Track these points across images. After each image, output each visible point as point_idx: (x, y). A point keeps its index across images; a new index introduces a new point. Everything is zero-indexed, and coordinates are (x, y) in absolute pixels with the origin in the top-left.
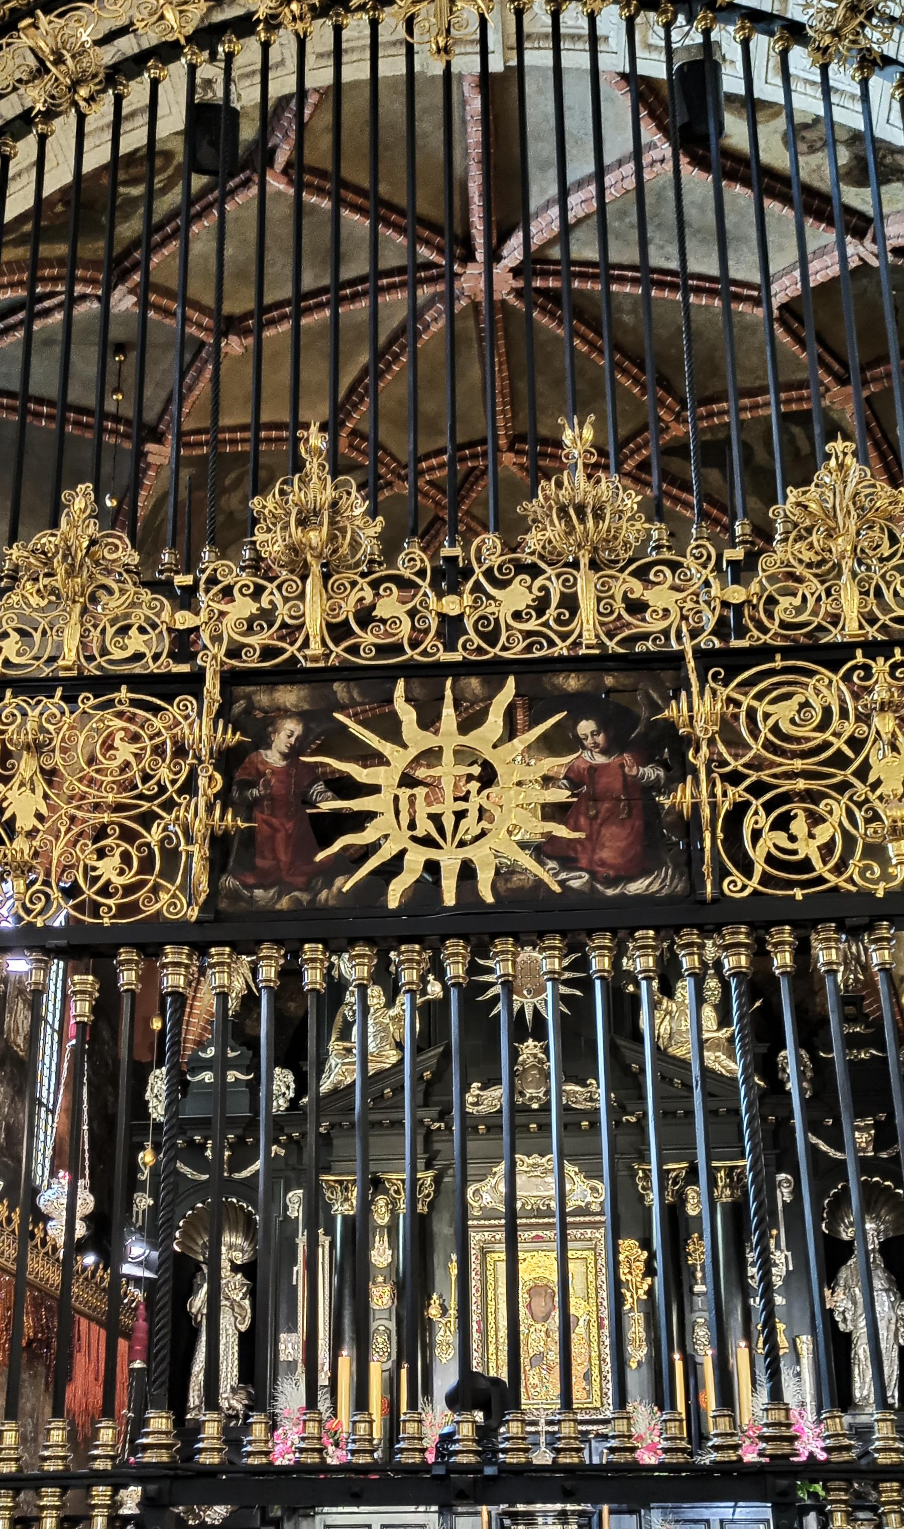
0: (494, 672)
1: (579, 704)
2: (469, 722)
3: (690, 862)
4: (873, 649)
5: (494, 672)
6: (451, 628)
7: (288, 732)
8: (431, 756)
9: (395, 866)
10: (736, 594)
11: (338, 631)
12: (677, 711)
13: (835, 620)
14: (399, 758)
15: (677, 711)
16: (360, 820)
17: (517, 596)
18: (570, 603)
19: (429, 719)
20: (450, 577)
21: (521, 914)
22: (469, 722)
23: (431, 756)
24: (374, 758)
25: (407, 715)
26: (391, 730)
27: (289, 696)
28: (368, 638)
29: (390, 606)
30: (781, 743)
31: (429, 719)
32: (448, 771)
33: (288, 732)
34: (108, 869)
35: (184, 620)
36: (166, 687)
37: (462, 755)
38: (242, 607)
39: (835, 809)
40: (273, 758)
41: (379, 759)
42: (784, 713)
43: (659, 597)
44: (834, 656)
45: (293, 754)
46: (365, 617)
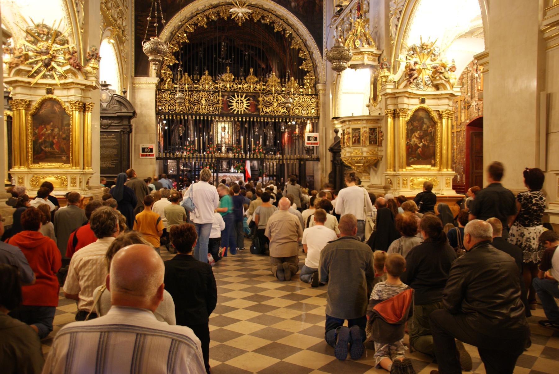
0: (244, 93)
1: (251, 96)
2: (242, 97)
3: (259, 111)
5: (244, 93)
6: (240, 88)
7: (226, 97)
8: (238, 100)
9: (235, 110)
10: (264, 87)
11: (230, 87)
12: (259, 99)
14: (236, 100)
15: (259, 99)
16: (232, 106)
17: (246, 86)
19: (238, 97)
20: (240, 84)
21: (245, 115)
22: (242, 97)
23: (238, 100)
24: (233, 100)
25: (236, 96)
26: (235, 97)
27: (226, 93)
28: (233, 88)
29: (235, 85)
30: (267, 101)
31: (238, 97)
32: (240, 102)
33: (226, 97)
34: (211, 109)
35: (217, 86)
36: (215, 92)
37: (241, 100)
38: (222, 85)
39: (271, 108)
40: (225, 99)
41: (233, 100)
42: (267, 99)
43: (258, 87)
44: (272, 94)
46: (232, 86)
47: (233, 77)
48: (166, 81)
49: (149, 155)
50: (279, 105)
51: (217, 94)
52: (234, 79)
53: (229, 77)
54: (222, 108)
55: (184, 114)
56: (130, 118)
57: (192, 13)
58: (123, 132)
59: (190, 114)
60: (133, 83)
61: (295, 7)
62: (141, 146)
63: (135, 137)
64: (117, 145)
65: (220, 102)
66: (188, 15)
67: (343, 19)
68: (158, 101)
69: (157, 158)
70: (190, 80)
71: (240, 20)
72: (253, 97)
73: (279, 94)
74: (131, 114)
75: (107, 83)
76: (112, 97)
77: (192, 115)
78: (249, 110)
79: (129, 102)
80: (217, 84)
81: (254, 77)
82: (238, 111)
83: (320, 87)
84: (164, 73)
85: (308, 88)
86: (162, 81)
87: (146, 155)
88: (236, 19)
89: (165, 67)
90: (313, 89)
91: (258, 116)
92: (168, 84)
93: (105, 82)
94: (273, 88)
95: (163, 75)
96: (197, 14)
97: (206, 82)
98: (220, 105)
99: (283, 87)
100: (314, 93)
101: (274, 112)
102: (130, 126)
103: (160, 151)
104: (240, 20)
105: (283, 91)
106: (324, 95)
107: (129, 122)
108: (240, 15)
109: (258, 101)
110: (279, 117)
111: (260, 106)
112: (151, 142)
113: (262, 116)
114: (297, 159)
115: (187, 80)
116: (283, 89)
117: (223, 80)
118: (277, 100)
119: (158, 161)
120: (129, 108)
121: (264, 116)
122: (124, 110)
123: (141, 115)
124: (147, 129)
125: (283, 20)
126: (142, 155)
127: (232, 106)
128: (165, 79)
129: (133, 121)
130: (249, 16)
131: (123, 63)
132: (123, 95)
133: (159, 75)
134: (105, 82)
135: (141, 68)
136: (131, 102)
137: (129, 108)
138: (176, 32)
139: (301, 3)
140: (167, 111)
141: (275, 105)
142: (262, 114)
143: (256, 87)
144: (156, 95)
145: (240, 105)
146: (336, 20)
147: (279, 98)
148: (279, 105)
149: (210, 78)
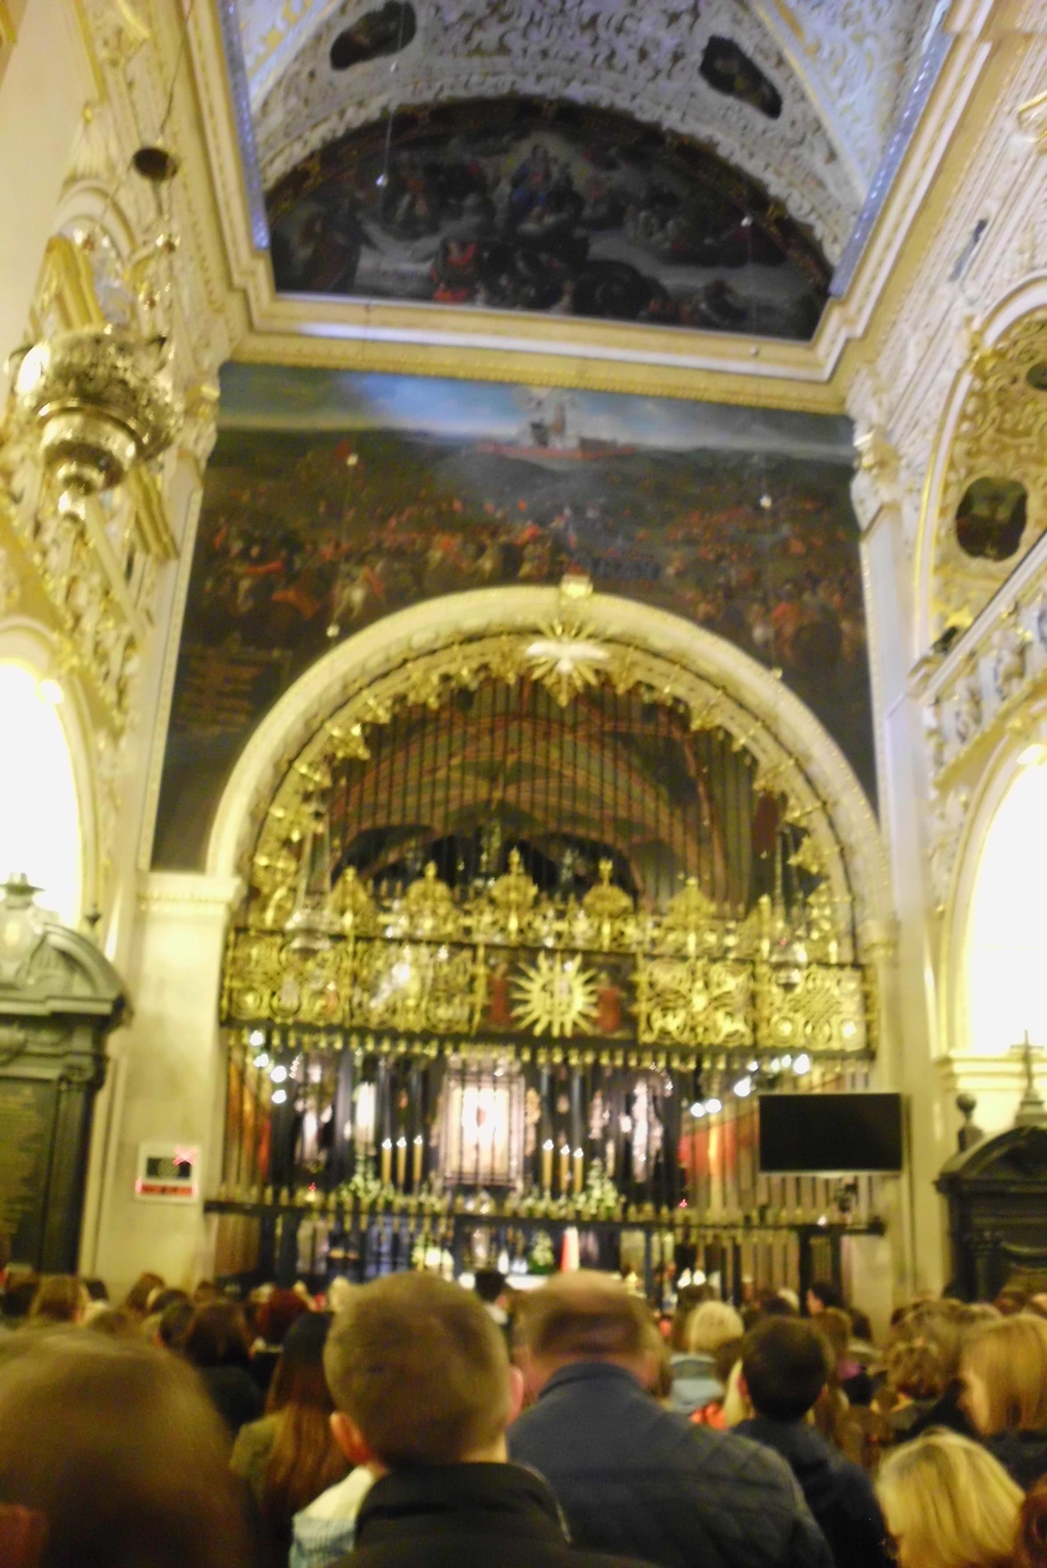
1: (601, 968)
4: (698, 958)
11: (521, 931)
13: (685, 944)
18: (599, 929)
35: (468, 922)
38: (487, 918)
43: (631, 931)
44: (685, 958)
45: (505, 975)
46: (530, 924)
47: (533, 890)
48: (269, 897)
49: (175, 1190)
50: (717, 1002)
51: (466, 954)
52: (537, 902)
53: (517, 888)
54: (486, 1011)
55: (331, 1029)
56: (102, 1025)
57: (388, 660)
58: (69, 1082)
59: (353, 1030)
60: (140, 898)
61: (766, 644)
62: (147, 1150)
63: (124, 1112)
64: (37, 1137)
65: (481, 986)
66: (375, 664)
67: (972, 654)
68: (232, 969)
69: (211, 1207)
70: (363, 897)
71: (564, 686)
72: (614, 970)
73: (714, 960)
74: (106, 1009)
75: (31, 882)
76: (43, 939)
77: (363, 1032)
78: (595, 1022)
79: (102, 962)
80: (468, 913)
81: (616, 892)
82: (550, 1025)
83: (873, 932)
84: (267, 867)
85: (825, 939)
86: (254, 895)
87: (164, 1190)
88: (549, 681)
89: (273, 845)
90: (847, 942)
91: (632, 1045)
92: (279, 908)
93: (23, 876)
94: (692, 940)
95: (261, 876)
96: (405, 661)
97: (425, 906)
98: (480, 997)
99: (728, 932)
100: (848, 957)
101: (693, 1029)
102: (100, 1060)
103: (224, 1177)
104: (564, 686)
105: (728, 950)
106: (894, 964)
107: (99, 1042)
108: (565, 667)
109: (631, 988)
110: (715, 1051)
111: (642, 1007)
112: (187, 1135)
113: (646, 1047)
114: (792, 1227)
115: (354, 894)
116: (731, 941)
117: (492, 901)
118: (707, 985)
119: (215, 1218)
120: (100, 980)
121: (655, 1049)
122: (80, 987)
123: (160, 1021)
124: (174, 1082)
125: (724, 688)
126: (146, 1189)
127: (526, 1002)
128: (266, 890)
129: (115, 1042)
130: (597, 672)
131: (102, 810)
132: (85, 929)
133: (245, 866)
134: (23, 876)
135: (178, 836)
136: (122, 969)
137: (100, 980)
138: (323, 722)
139: (789, 630)
140: (265, 1013)
141: (699, 1002)
142: (647, 1038)
143: (622, 933)
144: (226, 947)
145: (561, 998)
146: (927, 677)
147: (714, 978)
148: (717, 1002)
149: (441, 889)
